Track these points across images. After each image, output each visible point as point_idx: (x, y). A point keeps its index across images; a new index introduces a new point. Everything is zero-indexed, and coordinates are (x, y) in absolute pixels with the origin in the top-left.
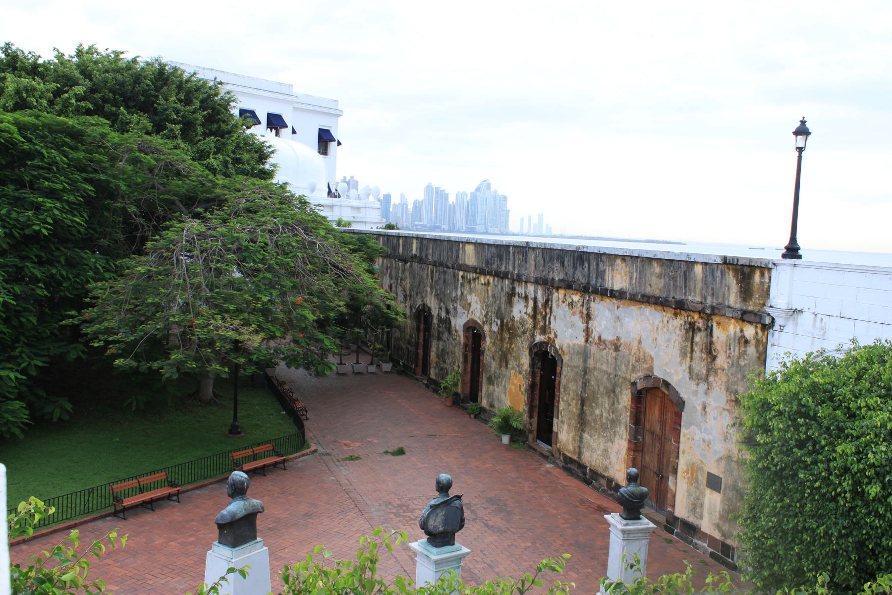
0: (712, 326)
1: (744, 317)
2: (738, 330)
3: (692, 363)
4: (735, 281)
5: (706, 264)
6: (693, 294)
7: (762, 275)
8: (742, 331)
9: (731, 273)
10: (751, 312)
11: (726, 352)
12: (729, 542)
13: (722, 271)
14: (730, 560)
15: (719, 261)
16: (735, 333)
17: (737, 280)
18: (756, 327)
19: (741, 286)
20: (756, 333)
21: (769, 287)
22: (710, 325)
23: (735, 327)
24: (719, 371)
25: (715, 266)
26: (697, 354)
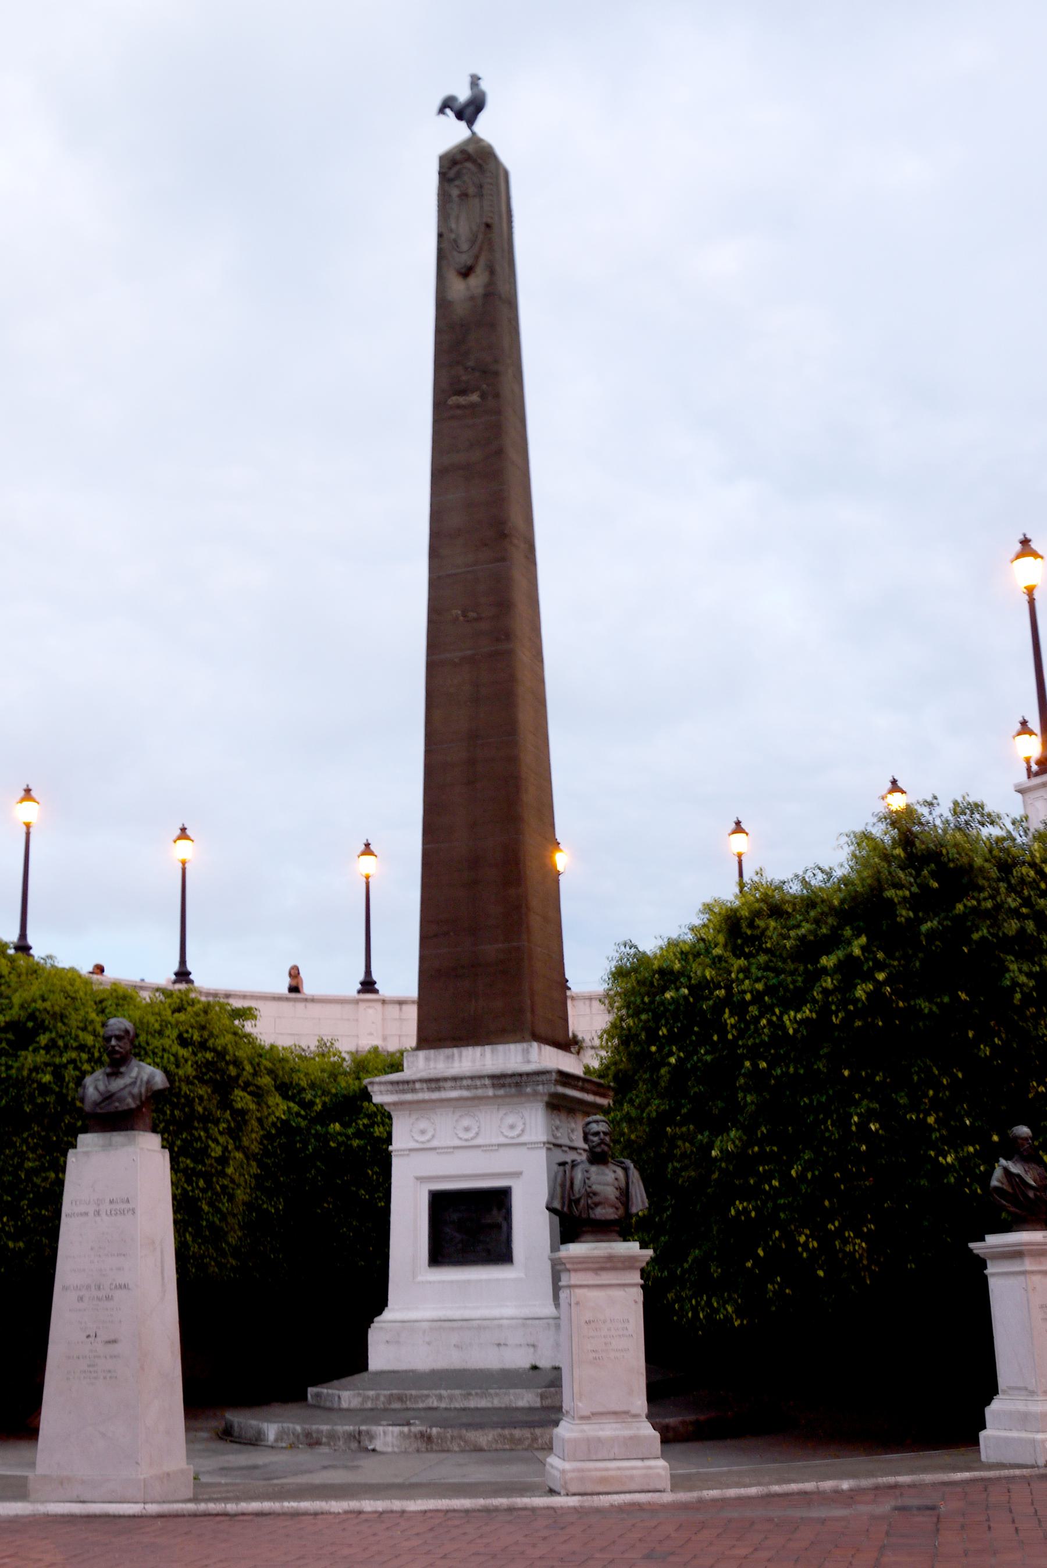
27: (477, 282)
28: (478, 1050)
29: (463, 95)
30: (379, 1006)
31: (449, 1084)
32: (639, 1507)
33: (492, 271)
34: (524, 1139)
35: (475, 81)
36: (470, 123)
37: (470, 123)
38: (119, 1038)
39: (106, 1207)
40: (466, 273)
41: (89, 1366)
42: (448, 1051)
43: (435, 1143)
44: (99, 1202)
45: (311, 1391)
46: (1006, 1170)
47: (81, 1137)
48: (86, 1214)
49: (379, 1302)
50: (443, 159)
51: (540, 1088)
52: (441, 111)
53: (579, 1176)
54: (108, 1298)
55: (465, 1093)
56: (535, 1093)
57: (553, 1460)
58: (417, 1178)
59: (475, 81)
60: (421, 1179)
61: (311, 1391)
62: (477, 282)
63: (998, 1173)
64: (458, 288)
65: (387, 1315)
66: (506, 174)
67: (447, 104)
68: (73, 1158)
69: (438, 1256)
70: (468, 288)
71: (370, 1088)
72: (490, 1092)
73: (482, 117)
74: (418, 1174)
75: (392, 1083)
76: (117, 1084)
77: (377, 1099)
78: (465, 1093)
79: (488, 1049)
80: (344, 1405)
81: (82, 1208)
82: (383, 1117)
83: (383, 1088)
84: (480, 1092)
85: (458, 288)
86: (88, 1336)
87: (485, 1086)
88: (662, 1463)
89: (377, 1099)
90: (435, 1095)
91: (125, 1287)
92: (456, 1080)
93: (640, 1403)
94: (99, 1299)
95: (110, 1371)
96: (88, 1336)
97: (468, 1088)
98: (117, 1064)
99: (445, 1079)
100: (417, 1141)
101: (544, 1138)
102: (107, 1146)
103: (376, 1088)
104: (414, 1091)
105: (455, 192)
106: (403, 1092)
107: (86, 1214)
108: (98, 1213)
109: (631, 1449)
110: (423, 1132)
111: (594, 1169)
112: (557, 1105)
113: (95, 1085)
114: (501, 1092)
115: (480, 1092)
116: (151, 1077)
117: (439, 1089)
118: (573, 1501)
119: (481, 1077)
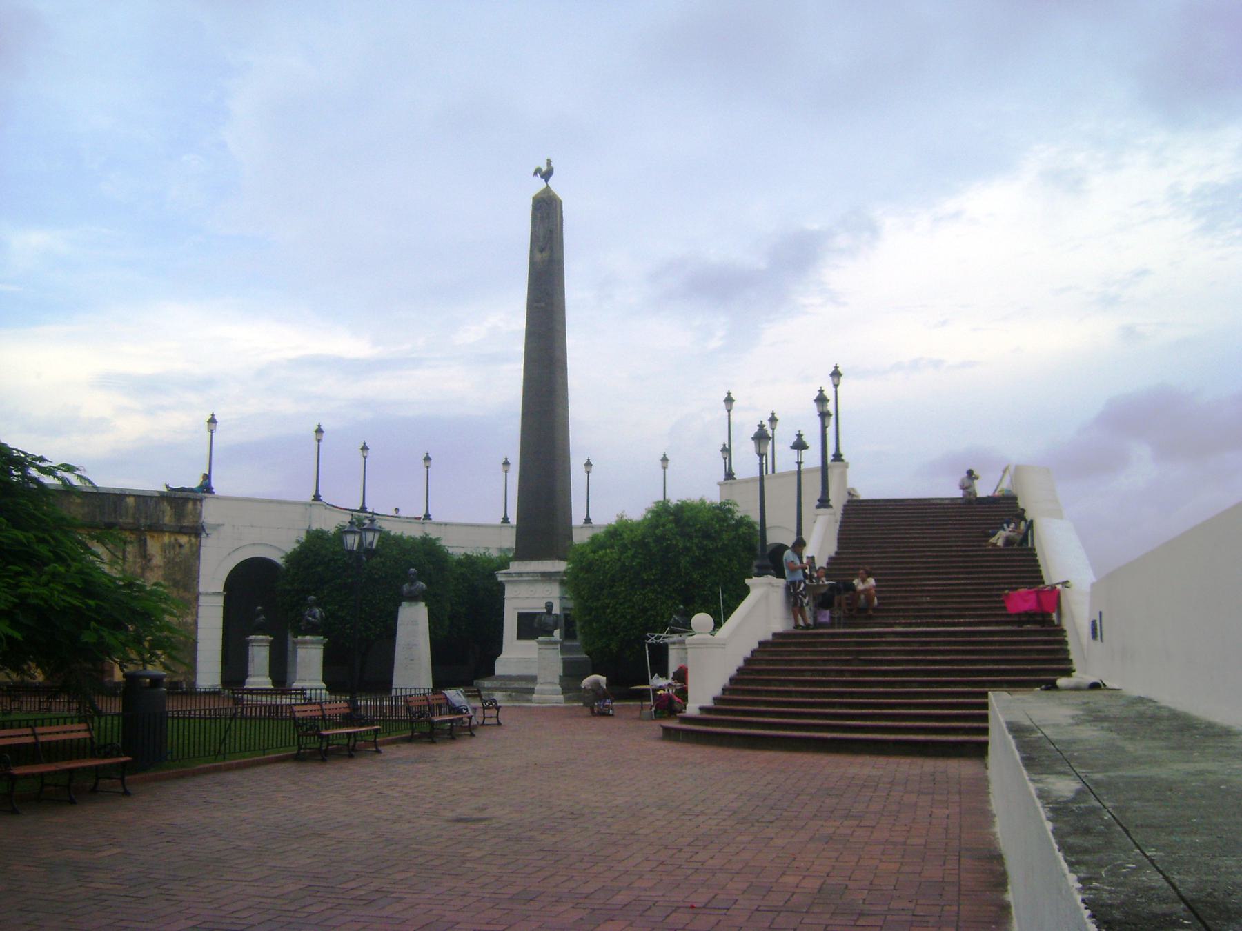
0: (145, 539)
1: (182, 531)
2: (173, 539)
3: (126, 567)
4: (169, 508)
5: (139, 496)
6: (124, 518)
7: (195, 504)
8: (176, 540)
9: (165, 504)
10: (185, 526)
11: (161, 555)
12: (175, 679)
13: (156, 502)
14: (180, 691)
15: (157, 495)
16: (170, 542)
17: (171, 509)
18: (190, 536)
19: (175, 511)
20: (190, 540)
21: (201, 512)
22: (143, 538)
23: (170, 537)
24: (155, 569)
25: (149, 500)
26: (130, 558)
27: (545, 255)
28: (537, 562)
29: (544, 168)
30: (510, 529)
31: (525, 575)
32: (554, 707)
33: (551, 249)
34: (551, 596)
35: (549, 162)
36: (546, 181)
37: (546, 181)
38: (413, 575)
40: (542, 250)
42: (525, 562)
43: (520, 596)
45: (475, 682)
46: (675, 619)
47: (403, 603)
49: (500, 652)
50: (533, 198)
51: (558, 578)
52: (535, 174)
53: (543, 618)
55: (531, 578)
56: (555, 581)
57: (534, 696)
59: (549, 162)
61: (475, 682)
62: (545, 255)
63: (672, 619)
64: (538, 256)
65: (502, 656)
66: (561, 202)
67: (538, 171)
68: (400, 610)
69: (521, 635)
70: (542, 257)
71: (497, 575)
72: (540, 578)
73: (552, 178)
75: (505, 574)
76: (413, 588)
77: (499, 579)
78: (531, 578)
79: (540, 562)
80: (486, 686)
82: (501, 587)
83: (502, 575)
84: (536, 578)
85: (538, 256)
87: (537, 576)
88: (562, 696)
89: (499, 579)
90: (520, 579)
91: (415, 645)
92: (528, 573)
93: (557, 681)
97: (532, 576)
98: (412, 582)
99: (524, 573)
101: (558, 595)
102: (410, 605)
103: (499, 575)
104: (513, 577)
105: (539, 215)
106: (509, 577)
108: (408, 625)
109: (554, 692)
110: (516, 592)
111: (547, 616)
112: (562, 583)
113: (406, 587)
114: (543, 578)
115: (536, 578)
116: (422, 586)
117: (522, 576)
118: (537, 705)
119: (536, 573)
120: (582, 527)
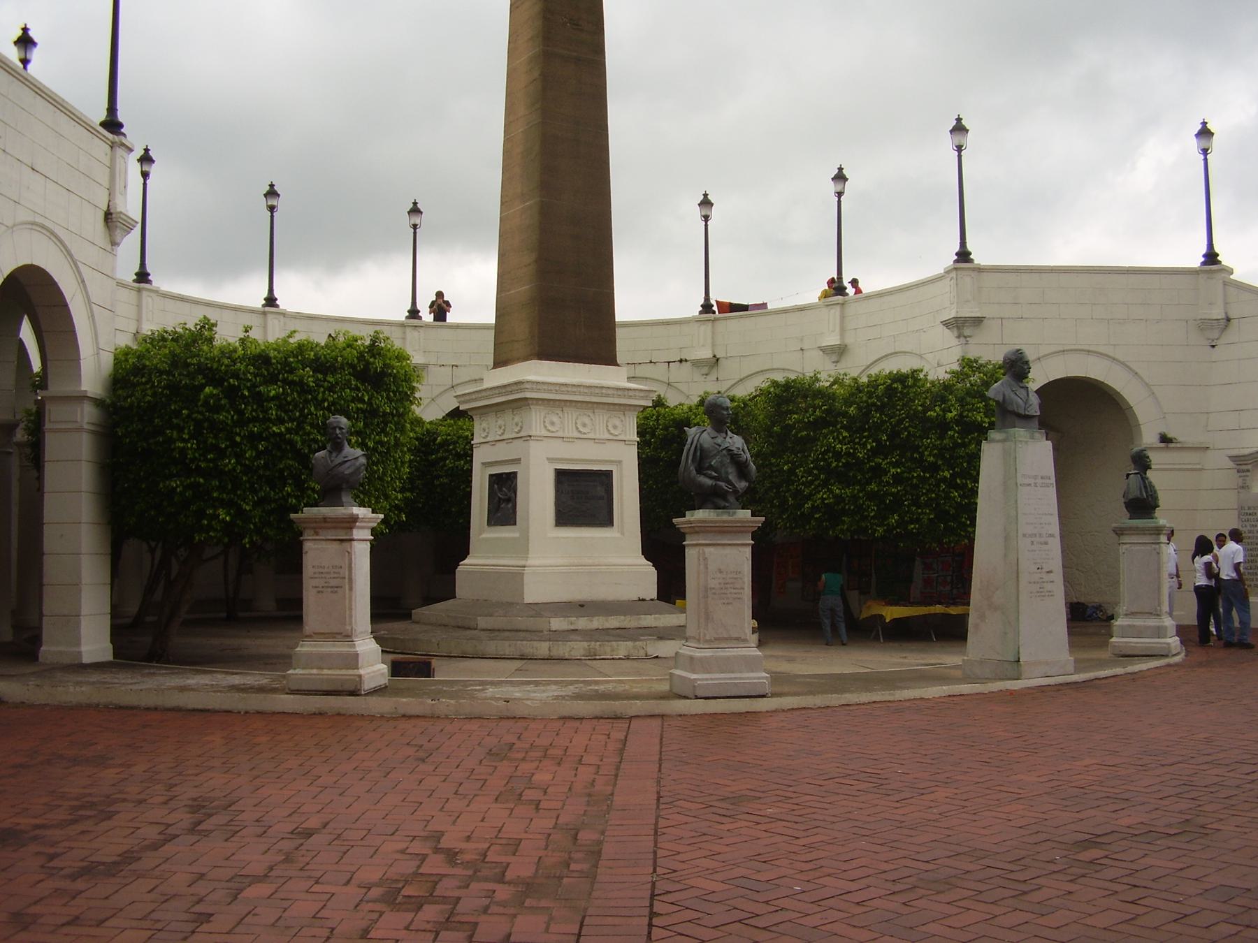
39: (1039, 481)
41: (1040, 588)
44: (1035, 477)
48: (1029, 485)
54: (1046, 543)
58: (548, 459)
60: (551, 460)
74: (551, 456)
81: (1027, 481)
86: (1038, 568)
94: (1041, 543)
95: (1050, 592)
96: (1038, 568)
100: (549, 430)
107: (1029, 485)
120: (264, 313)
